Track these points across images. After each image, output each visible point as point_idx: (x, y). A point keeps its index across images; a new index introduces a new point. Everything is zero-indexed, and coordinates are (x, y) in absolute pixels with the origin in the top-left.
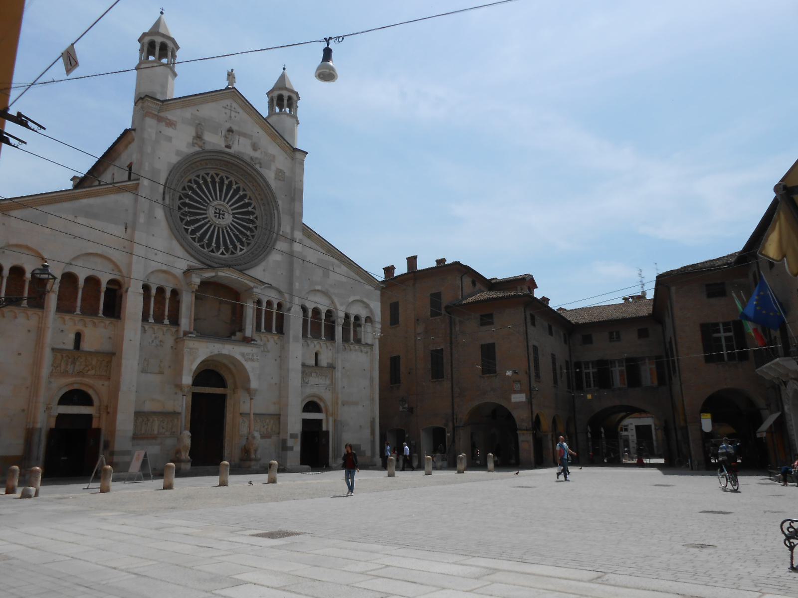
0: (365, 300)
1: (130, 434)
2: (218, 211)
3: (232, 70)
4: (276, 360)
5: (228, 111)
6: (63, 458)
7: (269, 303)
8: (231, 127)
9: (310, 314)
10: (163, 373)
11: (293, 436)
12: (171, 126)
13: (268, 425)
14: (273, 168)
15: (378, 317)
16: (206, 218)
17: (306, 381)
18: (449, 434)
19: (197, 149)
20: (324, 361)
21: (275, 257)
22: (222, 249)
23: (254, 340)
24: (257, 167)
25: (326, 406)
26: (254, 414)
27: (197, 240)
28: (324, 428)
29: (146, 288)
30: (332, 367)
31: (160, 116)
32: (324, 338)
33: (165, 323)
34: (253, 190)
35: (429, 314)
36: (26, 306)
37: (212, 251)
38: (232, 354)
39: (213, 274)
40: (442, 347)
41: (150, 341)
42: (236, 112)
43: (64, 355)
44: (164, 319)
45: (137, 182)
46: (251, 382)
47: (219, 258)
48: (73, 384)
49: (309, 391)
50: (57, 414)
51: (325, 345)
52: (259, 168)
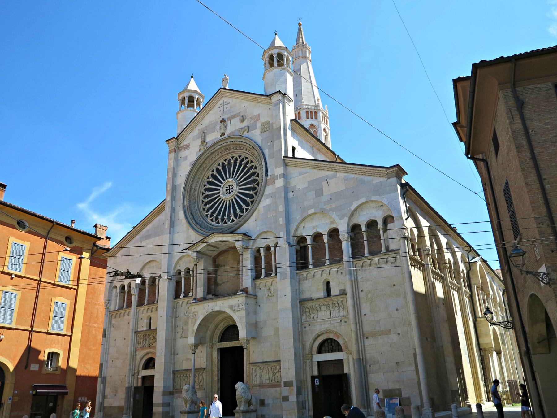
0: (374, 198)
3: (225, 75)
5: (221, 109)
12: (187, 148)
14: (259, 125)
16: (221, 198)
17: (315, 317)
19: (202, 151)
20: (335, 291)
21: (265, 202)
22: (232, 217)
24: (246, 134)
25: (345, 343)
27: (214, 220)
28: (346, 372)
31: (181, 147)
34: (250, 154)
37: (225, 223)
39: (205, 244)
42: (227, 104)
44: (190, 292)
48: (147, 354)
49: (318, 328)
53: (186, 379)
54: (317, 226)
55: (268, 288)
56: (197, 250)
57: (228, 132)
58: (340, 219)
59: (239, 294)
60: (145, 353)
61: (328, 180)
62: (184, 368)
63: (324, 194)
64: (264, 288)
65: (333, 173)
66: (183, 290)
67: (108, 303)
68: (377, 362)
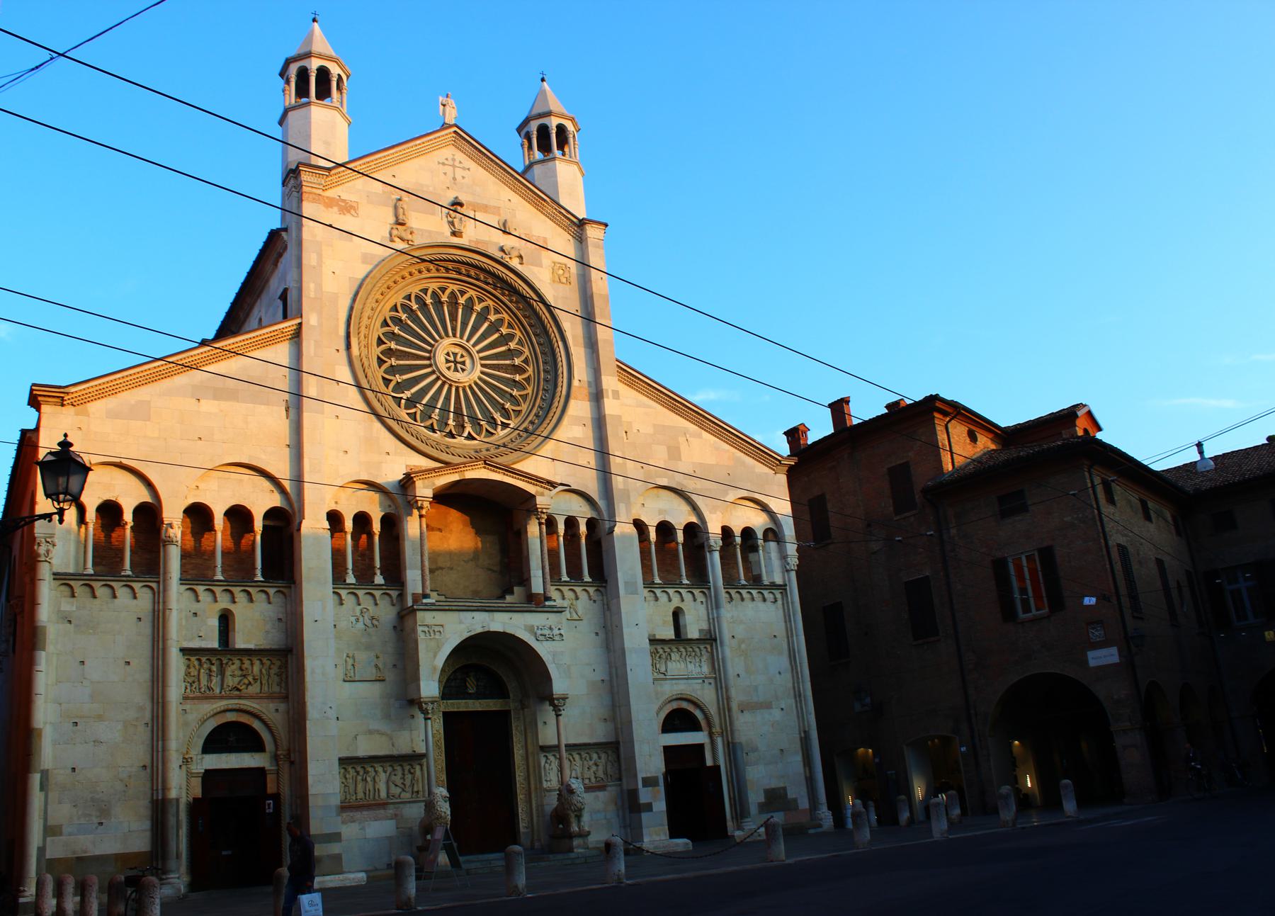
1: (336, 801)
2: (452, 358)
4: (597, 634)
5: (449, 170)
6: (224, 853)
7: (571, 522)
8: (456, 198)
9: (653, 535)
10: (383, 680)
11: (649, 782)
12: (349, 212)
13: (596, 765)
15: (789, 530)
18: (963, 749)
20: (693, 632)
23: (548, 599)
24: (514, 263)
26: (566, 746)
28: (709, 762)
29: (334, 518)
30: (710, 639)
31: (327, 197)
32: (685, 581)
33: (376, 582)
34: (514, 309)
35: (891, 509)
36: (129, 573)
37: (451, 435)
38: (509, 631)
39: (455, 477)
40: (927, 574)
41: (353, 619)
42: (464, 168)
43: (204, 659)
45: (298, 321)
46: (553, 681)
47: (463, 447)
50: (203, 771)
51: (690, 595)
52: (519, 268)
53: (369, 779)
54: (665, 511)
55: (570, 603)
56: (434, 484)
57: (472, 234)
58: (710, 513)
59: (549, 607)
60: (219, 710)
61: (688, 436)
62: (361, 752)
63: (683, 459)
64: (562, 601)
65: (697, 427)
66: (350, 565)
67: (54, 545)
68: (755, 750)
